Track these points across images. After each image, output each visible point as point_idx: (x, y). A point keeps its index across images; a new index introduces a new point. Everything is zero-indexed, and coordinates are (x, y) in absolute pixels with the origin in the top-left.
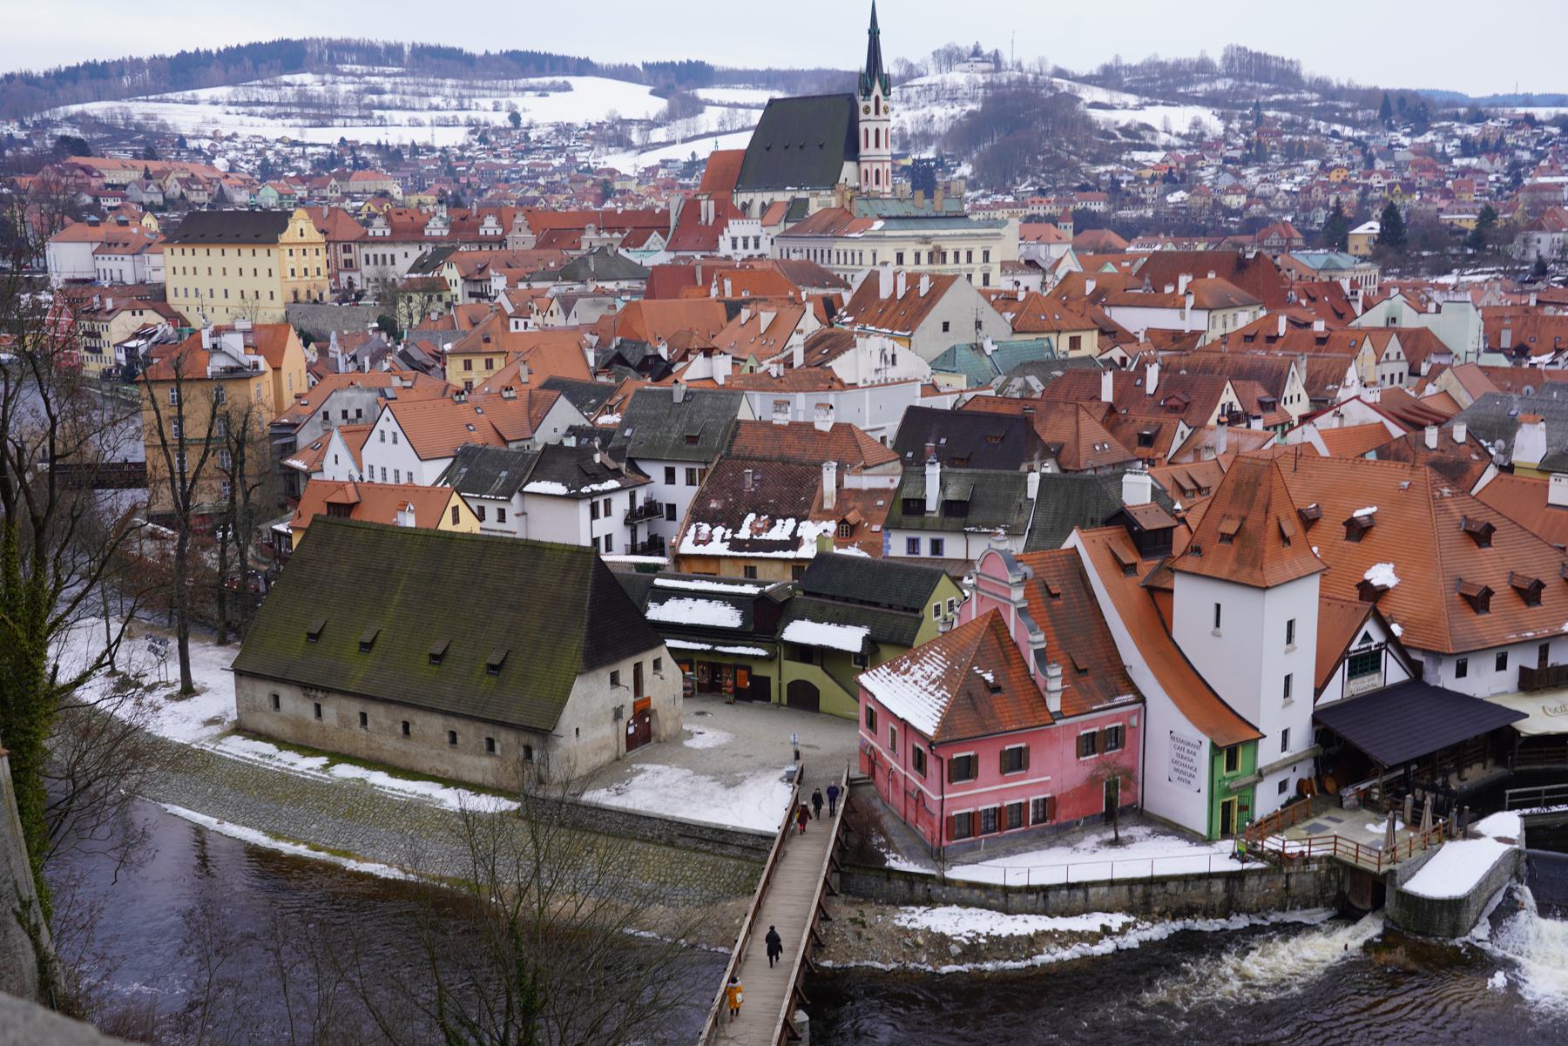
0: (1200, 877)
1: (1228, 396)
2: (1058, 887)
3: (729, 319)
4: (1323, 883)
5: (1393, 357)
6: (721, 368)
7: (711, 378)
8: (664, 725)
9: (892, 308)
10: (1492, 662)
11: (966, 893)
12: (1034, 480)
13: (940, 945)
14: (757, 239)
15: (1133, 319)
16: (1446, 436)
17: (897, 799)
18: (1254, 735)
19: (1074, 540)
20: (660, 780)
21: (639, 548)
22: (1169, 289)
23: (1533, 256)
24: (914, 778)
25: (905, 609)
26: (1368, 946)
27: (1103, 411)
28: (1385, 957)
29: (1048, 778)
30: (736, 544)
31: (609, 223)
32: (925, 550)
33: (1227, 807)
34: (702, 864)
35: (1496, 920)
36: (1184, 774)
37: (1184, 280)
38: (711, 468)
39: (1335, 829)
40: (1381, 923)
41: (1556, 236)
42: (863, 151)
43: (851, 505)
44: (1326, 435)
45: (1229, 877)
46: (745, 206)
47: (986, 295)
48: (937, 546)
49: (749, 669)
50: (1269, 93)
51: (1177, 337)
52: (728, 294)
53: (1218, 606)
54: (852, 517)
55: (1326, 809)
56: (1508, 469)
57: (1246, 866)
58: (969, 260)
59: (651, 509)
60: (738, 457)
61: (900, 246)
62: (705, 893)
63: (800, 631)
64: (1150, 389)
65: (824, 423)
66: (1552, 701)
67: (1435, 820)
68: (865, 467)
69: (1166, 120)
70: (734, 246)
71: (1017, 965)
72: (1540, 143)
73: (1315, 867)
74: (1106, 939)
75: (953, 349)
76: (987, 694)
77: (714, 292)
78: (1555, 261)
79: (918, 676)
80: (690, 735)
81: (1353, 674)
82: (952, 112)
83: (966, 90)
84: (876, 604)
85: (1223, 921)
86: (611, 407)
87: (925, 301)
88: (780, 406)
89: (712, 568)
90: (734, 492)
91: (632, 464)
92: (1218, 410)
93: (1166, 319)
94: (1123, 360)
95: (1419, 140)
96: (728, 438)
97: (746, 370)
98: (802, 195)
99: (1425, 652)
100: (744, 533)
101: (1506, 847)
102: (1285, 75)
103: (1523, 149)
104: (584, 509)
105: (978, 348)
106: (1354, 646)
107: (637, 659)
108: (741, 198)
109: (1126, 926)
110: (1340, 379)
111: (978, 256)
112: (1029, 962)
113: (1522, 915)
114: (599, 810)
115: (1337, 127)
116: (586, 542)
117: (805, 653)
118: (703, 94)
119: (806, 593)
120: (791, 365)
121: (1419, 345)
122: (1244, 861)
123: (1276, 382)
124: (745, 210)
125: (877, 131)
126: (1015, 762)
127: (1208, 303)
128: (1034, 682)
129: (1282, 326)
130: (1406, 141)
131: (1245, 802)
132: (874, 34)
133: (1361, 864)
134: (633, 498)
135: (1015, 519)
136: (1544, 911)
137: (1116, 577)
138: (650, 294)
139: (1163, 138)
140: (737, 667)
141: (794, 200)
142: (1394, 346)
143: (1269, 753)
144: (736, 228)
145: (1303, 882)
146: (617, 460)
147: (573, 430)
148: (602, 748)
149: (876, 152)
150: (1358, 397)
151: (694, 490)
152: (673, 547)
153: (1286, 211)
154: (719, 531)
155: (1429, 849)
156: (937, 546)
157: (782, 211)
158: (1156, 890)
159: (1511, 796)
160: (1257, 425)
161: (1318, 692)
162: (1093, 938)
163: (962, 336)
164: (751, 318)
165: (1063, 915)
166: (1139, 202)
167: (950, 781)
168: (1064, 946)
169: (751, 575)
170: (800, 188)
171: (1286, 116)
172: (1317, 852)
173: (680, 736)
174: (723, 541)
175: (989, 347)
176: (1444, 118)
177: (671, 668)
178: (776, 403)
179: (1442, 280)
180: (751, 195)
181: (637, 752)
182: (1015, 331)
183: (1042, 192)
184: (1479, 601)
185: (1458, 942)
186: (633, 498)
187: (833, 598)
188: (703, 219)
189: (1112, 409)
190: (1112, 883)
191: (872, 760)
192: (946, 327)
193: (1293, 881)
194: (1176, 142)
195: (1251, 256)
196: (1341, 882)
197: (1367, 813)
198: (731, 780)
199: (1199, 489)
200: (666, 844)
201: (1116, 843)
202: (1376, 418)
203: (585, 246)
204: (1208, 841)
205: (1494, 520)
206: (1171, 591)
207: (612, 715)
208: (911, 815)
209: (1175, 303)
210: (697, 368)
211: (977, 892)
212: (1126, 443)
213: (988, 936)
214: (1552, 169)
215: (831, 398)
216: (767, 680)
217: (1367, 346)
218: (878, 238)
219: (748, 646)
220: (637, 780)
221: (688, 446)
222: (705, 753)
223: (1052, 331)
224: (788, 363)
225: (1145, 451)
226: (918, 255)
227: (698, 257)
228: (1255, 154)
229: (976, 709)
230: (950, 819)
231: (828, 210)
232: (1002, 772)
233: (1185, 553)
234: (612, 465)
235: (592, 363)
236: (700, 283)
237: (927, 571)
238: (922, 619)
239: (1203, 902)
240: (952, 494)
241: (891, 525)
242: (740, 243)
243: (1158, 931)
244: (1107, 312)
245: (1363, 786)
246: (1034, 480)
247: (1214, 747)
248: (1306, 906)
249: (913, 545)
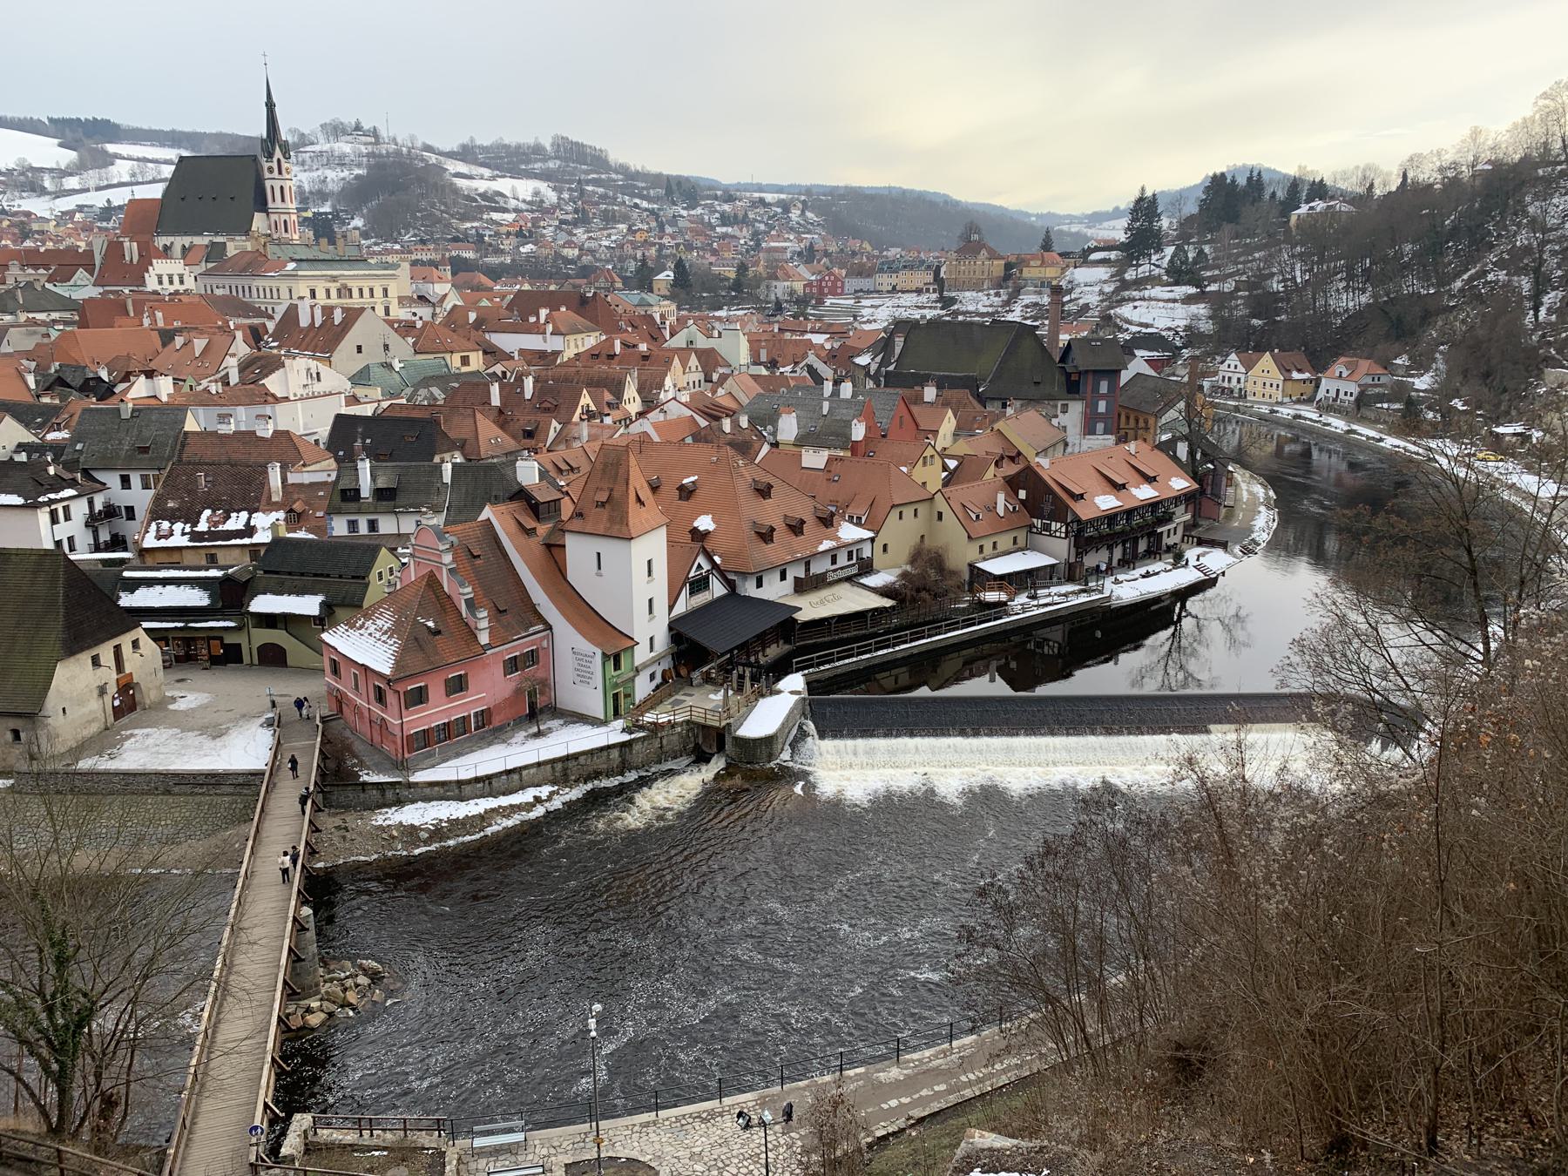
0: (602, 749)
1: (586, 400)
2: (501, 773)
3: (164, 345)
4: (684, 740)
5: (693, 369)
6: (164, 387)
7: (155, 397)
8: (149, 695)
9: (311, 335)
10: (778, 575)
11: (428, 791)
12: (447, 469)
13: (411, 834)
14: (181, 277)
15: (509, 342)
16: (735, 424)
17: (364, 728)
18: (631, 643)
19: (487, 513)
20: (150, 741)
21: (102, 546)
22: (532, 319)
23: (773, 298)
24: (376, 709)
25: (353, 577)
26: (717, 777)
27: (495, 413)
28: (728, 783)
30: (195, 536)
31: (32, 259)
32: (363, 529)
33: (616, 696)
34: (199, 804)
35: (793, 746)
36: (584, 677)
37: (543, 312)
38: (165, 473)
39: (689, 701)
40: (723, 760)
41: (786, 284)
42: (270, 205)
43: (296, 496)
44: (656, 426)
45: (623, 745)
46: (167, 248)
47: (390, 323)
48: (373, 525)
49: (221, 639)
50: (587, 172)
51: (542, 355)
52: (161, 324)
53: (599, 554)
54: (297, 506)
55: (680, 689)
56: (775, 445)
57: (633, 736)
58: (372, 296)
59: (110, 512)
60: (189, 463)
61: (312, 284)
62: (205, 827)
63: (263, 604)
64: (528, 395)
65: (265, 431)
66: (814, 597)
67: (752, 685)
68: (304, 465)
69: (514, 189)
70: (160, 282)
71: (473, 837)
72: (770, 218)
73: (679, 729)
74: (538, 806)
75: (367, 366)
76: (431, 637)
77: (146, 322)
78: (786, 301)
79: (372, 629)
80: (174, 699)
81: (692, 593)
82: (342, 175)
83: (352, 157)
84: (328, 576)
85: (620, 778)
86: (59, 424)
87: (340, 329)
88: (224, 418)
89: (176, 557)
90: (189, 492)
91: (86, 473)
92: (579, 411)
93: (533, 342)
94: (504, 373)
95: (692, 212)
96: (178, 447)
97: (186, 389)
98: (219, 239)
99: (736, 573)
100: (203, 526)
101: (796, 697)
102: (598, 161)
103: (760, 222)
104: (43, 516)
105: (389, 366)
106: (692, 574)
107: (115, 642)
108: (162, 241)
109: (552, 794)
110: (661, 386)
111: (378, 292)
112: (482, 834)
113: (809, 739)
114: (92, 774)
115: (637, 201)
116: (50, 546)
117: (269, 620)
118: (111, 148)
119: (266, 572)
120: (228, 384)
121: (709, 360)
122: (631, 733)
123: (618, 390)
124: (166, 252)
125: (282, 188)
126: (457, 686)
127: (563, 330)
129: (618, 349)
130: (684, 213)
131: (628, 691)
132: (270, 106)
133: (709, 723)
134: (91, 503)
135: (435, 500)
136: (822, 736)
137: (523, 539)
138: (83, 324)
139: (513, 203)
140: (210, 638)
141: (213, 244)
142: (693, 361)
143: (642, 655)
144: (160, 267)
145: (671, 740)
146: (71, 471)
147: (21, 447)
148: (90, 722)
149: (283, 206)
150: (674, 399)
151: (151, 493)
152: (136, 542)
153: (608, 262)
154: (178, 527)
155: (750, 705)
156: (373, 525)
157: (204, 252)
158: (571, 764)
159: (797, 663)
160: (608, 421)
161: (671, 608)
162: (529, 807)
163: (373, 356)
164: (185, 344)
165: (504, 794)
166: (499, 252)
167: (407, 708)
168: (508, 817)
169: (212, 561)
170: (217, 234)
171: (601, 190)
172: (679, 719)
173: (163, 703)
174: (183, 534)
175: (397, 366)
176: (708, 197)
177: (149, 646)
178: (219, 415)
179: (717, 314)
180: (171, 239)
181: (124, 720)
182: (416, 352)
183: (423, 242)
184: (766, 536)
185: (772, 764)
186: (91, 503)
187: (290, 574)
188: (127, 258)
189: (500, 411)
190: (539, 764)
191: (339, 700)
192: (359, 349)
193: (665, 742)
194: (523, 206)
195: (590, 295)
196: (696, 737)
197: (709, 687)
198: (216, 732)
199: (572, 469)
200: (163, 794)
201: (539, 734)
202: (689, 413)
203: (10, 281)
204: (604, 723)
205: (772, 481)
206: (564, 546)
207: (96, 693)
208: (377, 738)
209: (538, 329)
210: (140, 388)
211: (436, 789)
212: (514, 437)
213: (449, 821)
214: (779, 237)
215: (268, 410)
217: (676, 361)
218: (292, 276)
219: (218, 620)
220: (127, 744)
221: (141, 456)
222: (186, 713)
223: (446, 352)
224: (225, 381)
225: (530, 443)
226: (328, 291)
227: (127, 291)
228: (582, 219)
229: (422, 649)
231: (244, 253)
232: (447, 695)
233: (571, 518)
234: (67, 476)
235: (33, 386)
236: (132, 314)
237: (369, 546)
238: (367, 585)
239: (605, 766)
240: (382, 483)
241: (333, 511)
242: (165, 279)
243: (575, 793)
244: (487, 336)
245: (704, 669)
246: (447, 469)
247: (604, 654)
248: (675, 758)
249: (353, 525)
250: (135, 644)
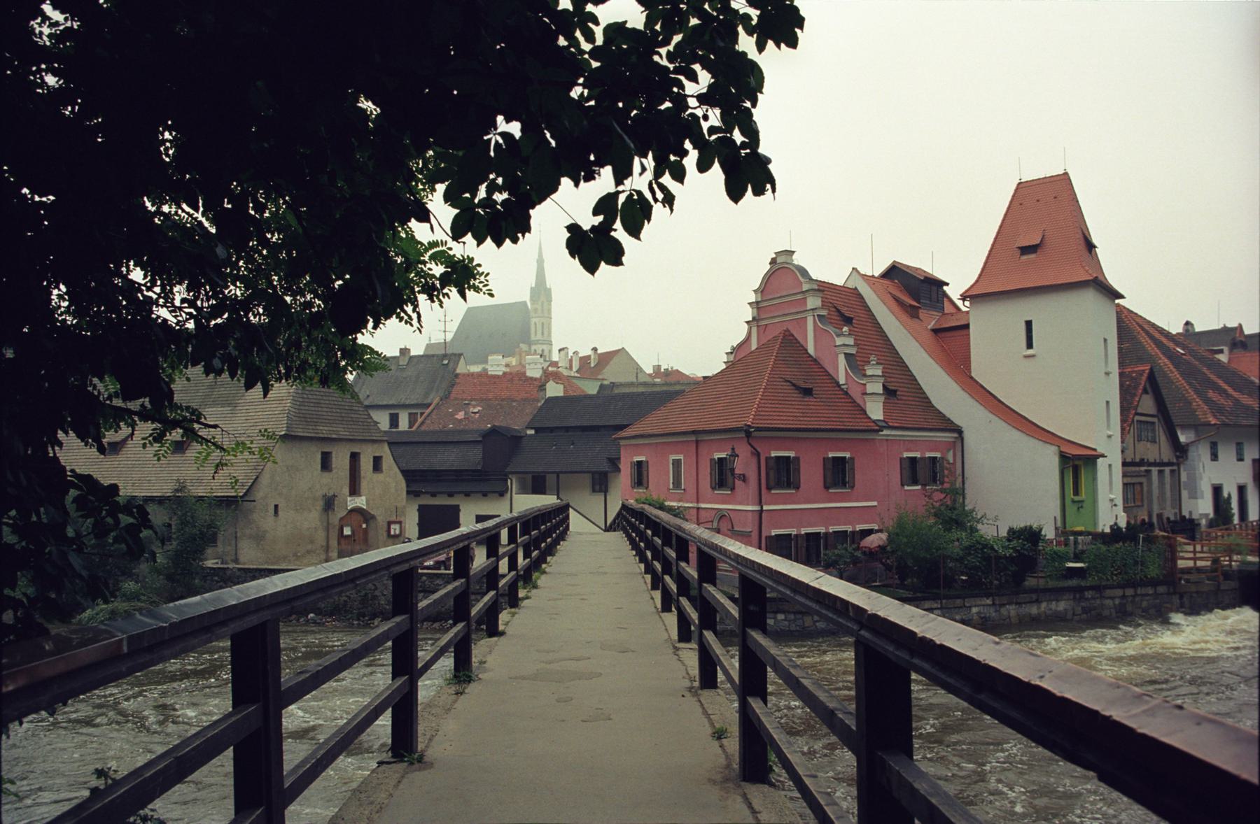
29: (875, 503)
53: (1029, 324)
119: (537, 430)
128: (846, 393)
206: (967, 326)
207: (320, 504)
232: (827, 487)
250: (377, 464)
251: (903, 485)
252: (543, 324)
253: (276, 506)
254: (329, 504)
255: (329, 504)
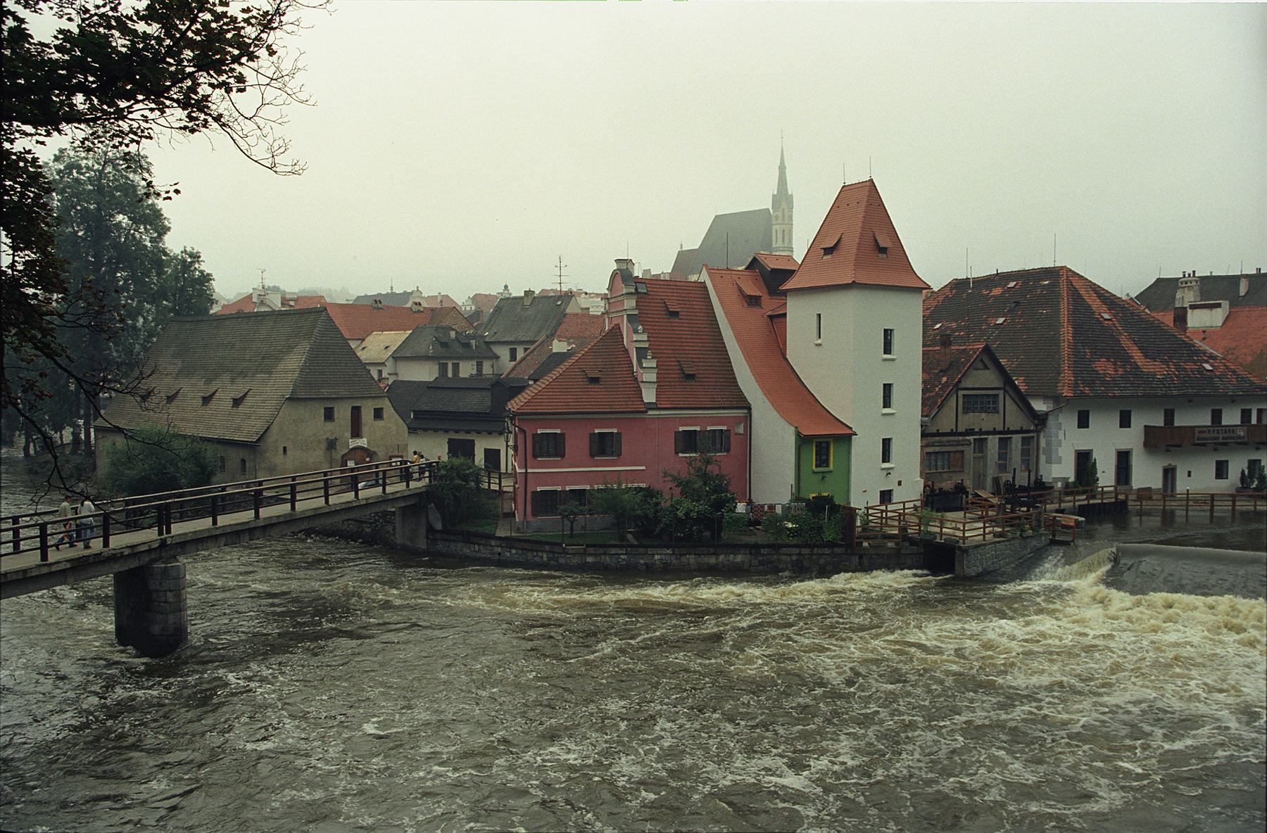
29: (644, 468)
132: (782, 168)
167: (535, 456)
206: (785, 315)
207: (324, 446)
216: (499, 450)
230: (535, 493)
232: (592, 455)
250: (378, 414)
251: (677, 453)
252: (784, 231)
253: (285, 449)
254: (331, 444)
255: (331, 444)
